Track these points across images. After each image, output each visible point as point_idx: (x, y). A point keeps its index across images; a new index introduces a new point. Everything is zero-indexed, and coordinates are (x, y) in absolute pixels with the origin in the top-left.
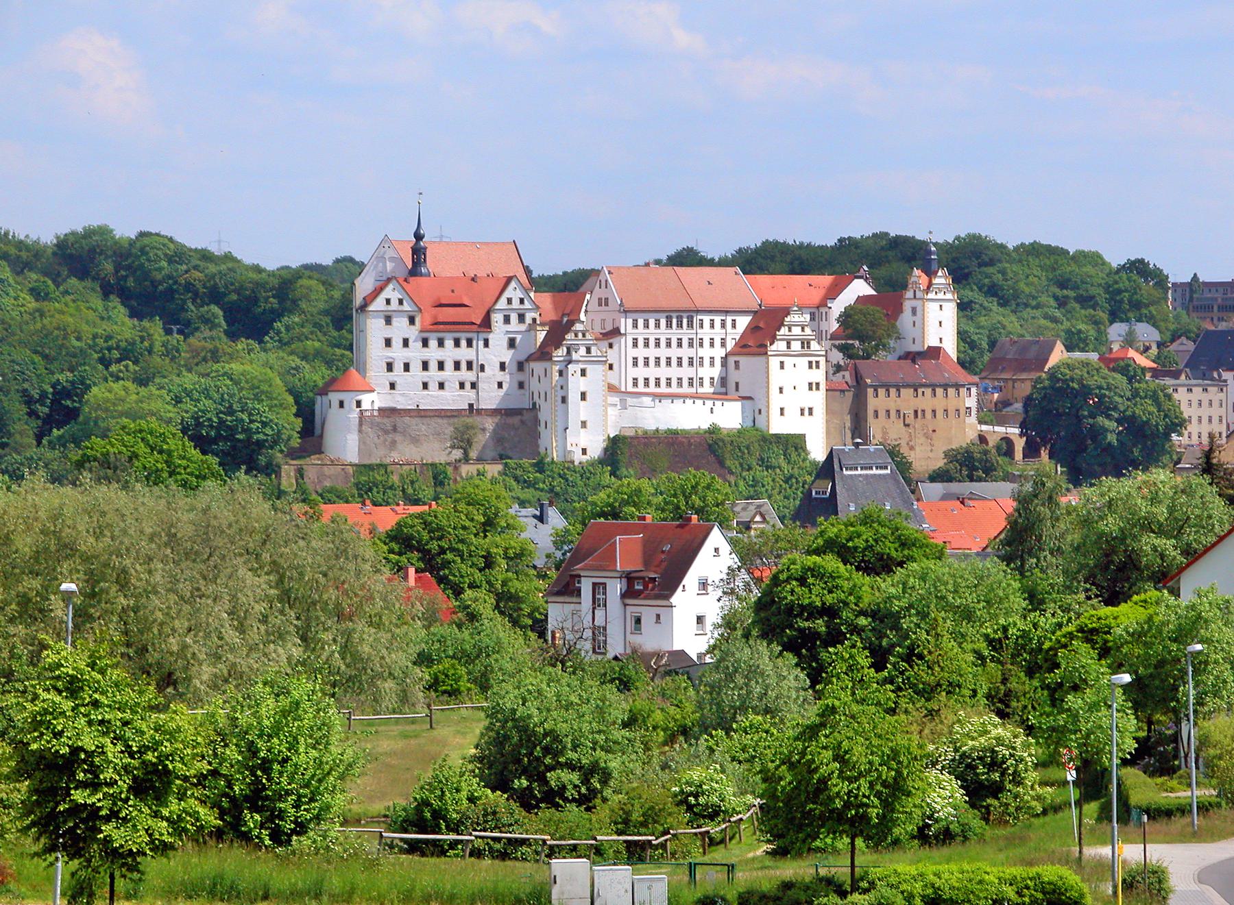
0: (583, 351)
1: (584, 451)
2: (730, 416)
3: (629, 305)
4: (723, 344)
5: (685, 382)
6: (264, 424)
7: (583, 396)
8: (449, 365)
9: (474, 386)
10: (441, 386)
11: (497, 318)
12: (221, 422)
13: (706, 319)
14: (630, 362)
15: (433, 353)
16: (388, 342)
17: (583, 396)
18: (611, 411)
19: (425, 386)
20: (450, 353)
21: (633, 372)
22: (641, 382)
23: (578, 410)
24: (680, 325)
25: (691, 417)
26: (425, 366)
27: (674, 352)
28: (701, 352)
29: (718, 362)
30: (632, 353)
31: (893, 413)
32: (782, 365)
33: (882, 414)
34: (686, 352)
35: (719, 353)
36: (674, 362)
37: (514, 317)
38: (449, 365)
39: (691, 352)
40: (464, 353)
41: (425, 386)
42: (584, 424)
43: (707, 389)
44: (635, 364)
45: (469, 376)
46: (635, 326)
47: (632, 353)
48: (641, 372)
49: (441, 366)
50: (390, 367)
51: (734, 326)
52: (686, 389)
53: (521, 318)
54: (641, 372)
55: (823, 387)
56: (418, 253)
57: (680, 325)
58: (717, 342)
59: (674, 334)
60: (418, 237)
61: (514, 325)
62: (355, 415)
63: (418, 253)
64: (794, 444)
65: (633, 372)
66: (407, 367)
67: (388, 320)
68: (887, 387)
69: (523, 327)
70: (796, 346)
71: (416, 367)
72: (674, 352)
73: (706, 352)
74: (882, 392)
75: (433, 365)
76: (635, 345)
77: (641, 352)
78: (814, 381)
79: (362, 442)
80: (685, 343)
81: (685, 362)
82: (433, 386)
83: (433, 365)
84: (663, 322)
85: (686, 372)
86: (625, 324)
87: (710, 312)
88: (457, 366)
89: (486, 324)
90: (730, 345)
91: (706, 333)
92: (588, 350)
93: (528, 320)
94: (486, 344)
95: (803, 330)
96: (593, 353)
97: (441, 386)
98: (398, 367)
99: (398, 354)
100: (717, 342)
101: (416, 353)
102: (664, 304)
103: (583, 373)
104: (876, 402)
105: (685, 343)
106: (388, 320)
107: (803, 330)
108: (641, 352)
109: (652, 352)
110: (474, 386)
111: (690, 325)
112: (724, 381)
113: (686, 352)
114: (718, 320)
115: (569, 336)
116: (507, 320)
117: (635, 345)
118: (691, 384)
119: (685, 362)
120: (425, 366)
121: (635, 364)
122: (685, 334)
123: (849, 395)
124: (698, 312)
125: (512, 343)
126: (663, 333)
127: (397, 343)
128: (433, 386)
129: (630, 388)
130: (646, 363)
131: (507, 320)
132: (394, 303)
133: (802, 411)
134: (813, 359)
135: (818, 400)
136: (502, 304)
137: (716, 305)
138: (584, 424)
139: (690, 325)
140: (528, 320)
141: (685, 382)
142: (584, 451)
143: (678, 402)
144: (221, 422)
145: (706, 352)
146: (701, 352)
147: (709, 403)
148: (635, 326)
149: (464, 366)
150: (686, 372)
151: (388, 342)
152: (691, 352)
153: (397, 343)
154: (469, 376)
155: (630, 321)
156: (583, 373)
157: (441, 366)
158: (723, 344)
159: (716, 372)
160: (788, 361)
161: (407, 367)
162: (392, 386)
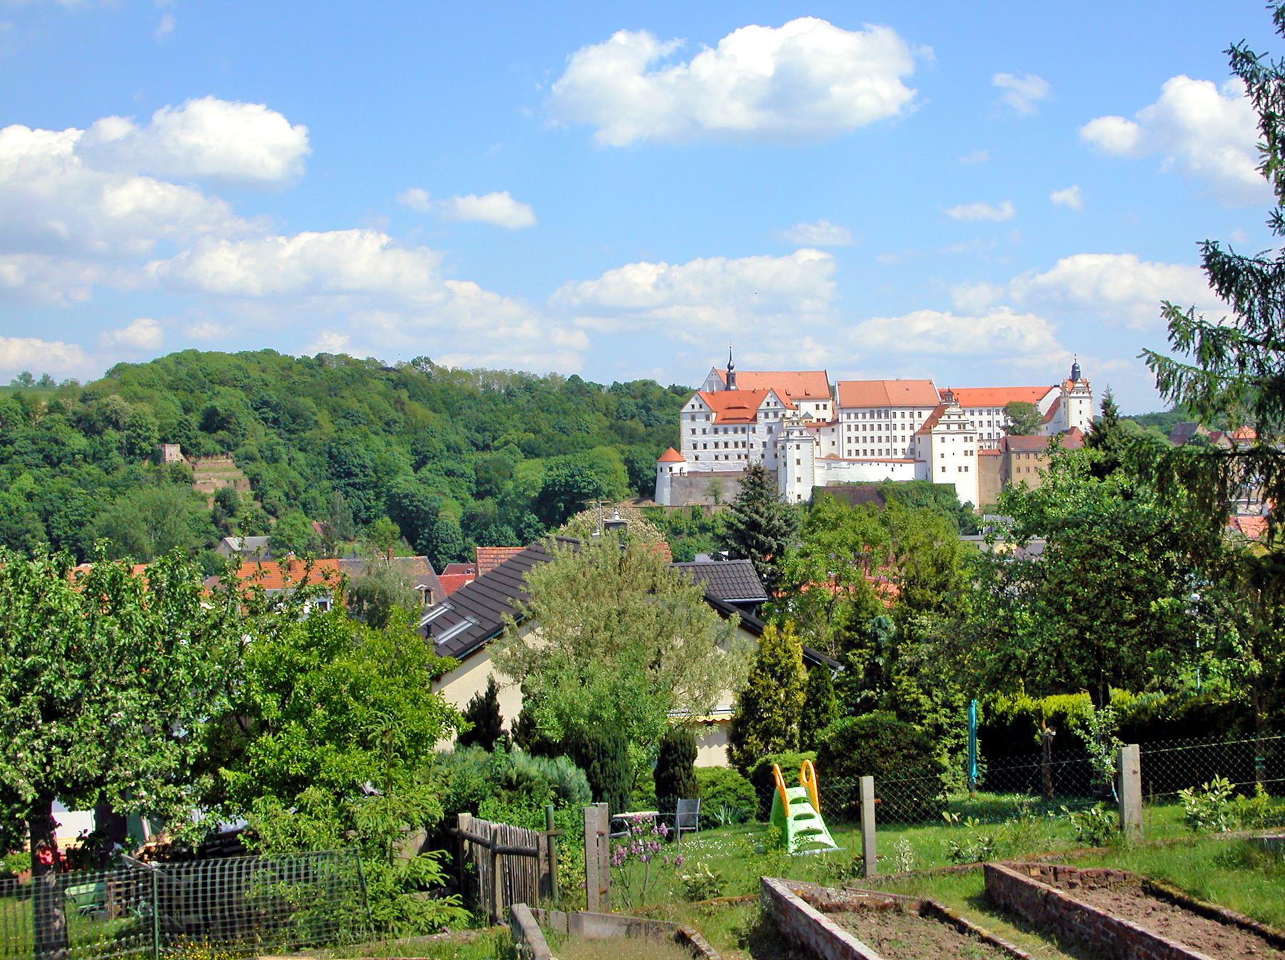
0: (796, 434)
1: (799, 497)
2: (906, 473)
3: (843, 405)
4: (912, 427)
5: (884, 452)
6: (589, 483)
7: (798, 462)
8: (731, 445)
9: (746, 457)
10: (727, 457)
11: (761, 415)
12: (567, 482)
13: (899, 413)
14: (846, 440)
15: (721, 437)
16: (694, 431)
17: (798, 462)
18: (817, 471)
19: (717, 458)
20: (731, 437)
21: (847, 446)
22: (853, 453)
23: (793, 471)
24: (879, 416)
25: (874, 474)
26: (716, 445)
28: (894, 433)
29: (908, 439)
30: (849, 434)
31: (1032, 470)
33: (1023, 470)
35: (908, 433)
36: (876, 439)
37: (771, 415)
38: (731, 445)
39: (888, 433)
40: (740, 437)
41: (717, 458)
42: (799, 479)
43: (900, 455)
45: (741, 450)
46: (849, 417)
47: (849, 434)
48: (853, 446)
49: (726, 445)
50: (695, 447)
51: (920, 415)
52: (884, 456)
53: (776, 415)
54: (853, 446)
55: (975, 453)
56: (730, 378)
57: (879, 416)
58: (907, 427)
59: (876, 421)
60: (730, 368)
61: (771, 419)
62: (668, 476)
63: (730, 378)
64: (949, 490)
65: (847, 446)
66: (705, 446)
67: (693, 419)
68: (1027, 453)
69: (777, 420)
70: (954, 428)
71: (711, 447)
73: (898, 433)
74: (1023, 456)
75: (721, 445)
76: (849, 428)
77: (853, 434)
78: (969, 449)
79: (672, 494)
82: (722, 458)
83: (721, 445)
84: (868, 415)
85: (884, 446)
86: (843, 417)
87: (901, 407)
88: (736, 445)
89: (755, 419)
90: (917, 428)
91: (898, 421)
93: (780, 415)
94: (754, 431)
97: (727, 457)
98: (700, 446)
99: (700, 438)
100: (907, 427)
101: (710, 438)
102: (868, 403)
103: (798, 447)
104: (1015, 462)
106: (693, 419)
108: (853, 434)
109: (861, 434)
110: (746, 457)
111: (886, 415)
112: (912, 451)
113: (884, 433)
114: (907, 413)
116: (767, 416)
117: (849, 428)
118: (888, 453)
119: (884, 439)
120: (716, 445)
123: (1000, 458)
125: (770, 430)
127: (699, 432)
128: (722, 458)
129: (846, 457)
130: (857, 441)
131: (767, 416)
132: (697, 407)
135: (972, 462)
136: (763, 406)
137: (907, 403)
138: (799, 479)
139: (886, 415)
140: (780, 415)
141: (884, 452)
142: (799, 497)
143: (867, 465)
144: (567, 482)
145: (898, 433)
146: (894, 433)
147: (890, 465)
148: (849, 417)
149: (740, 444)
150: (884, 446)
151: (694, 431)
152: (888, 433)
153: (699, 432)
154: (743, 451)
155: (845, 416)
156: (798, 447)
157: (726, 445)
158: (912, 427)
159: (907, 445)
161: (705, 446)
162: (697, 458)
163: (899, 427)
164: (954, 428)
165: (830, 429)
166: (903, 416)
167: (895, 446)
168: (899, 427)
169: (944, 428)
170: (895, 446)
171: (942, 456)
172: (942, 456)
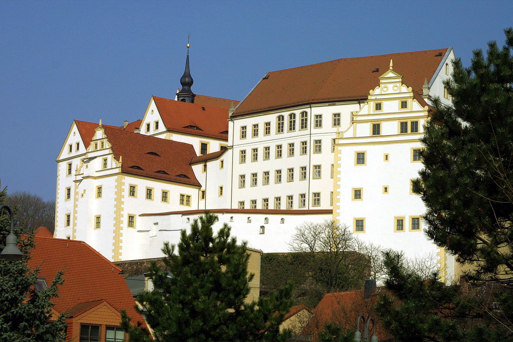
13: (327, 112)
28: (316, 159)
32: (361, 158)
34: (297, 161)
59: (286, 138)
70: (390, 128)
77: (249, 168)
85: (297, 187)
91: (326, 132)
95: (404, 105)
96: (109, 166)
107: (404, 105)
108: (249, 168)
113: (297, 161)
122: (297, 136)
124: (310, 104)
126: (274, 139)
133: (400, 225)
146: (316, 159)
148: (244, 135)
164: (390, 128)
165: (218, 162)
169: (366, 129)
170: (316, 186)
171: (358, 194)
172: (358, 194)
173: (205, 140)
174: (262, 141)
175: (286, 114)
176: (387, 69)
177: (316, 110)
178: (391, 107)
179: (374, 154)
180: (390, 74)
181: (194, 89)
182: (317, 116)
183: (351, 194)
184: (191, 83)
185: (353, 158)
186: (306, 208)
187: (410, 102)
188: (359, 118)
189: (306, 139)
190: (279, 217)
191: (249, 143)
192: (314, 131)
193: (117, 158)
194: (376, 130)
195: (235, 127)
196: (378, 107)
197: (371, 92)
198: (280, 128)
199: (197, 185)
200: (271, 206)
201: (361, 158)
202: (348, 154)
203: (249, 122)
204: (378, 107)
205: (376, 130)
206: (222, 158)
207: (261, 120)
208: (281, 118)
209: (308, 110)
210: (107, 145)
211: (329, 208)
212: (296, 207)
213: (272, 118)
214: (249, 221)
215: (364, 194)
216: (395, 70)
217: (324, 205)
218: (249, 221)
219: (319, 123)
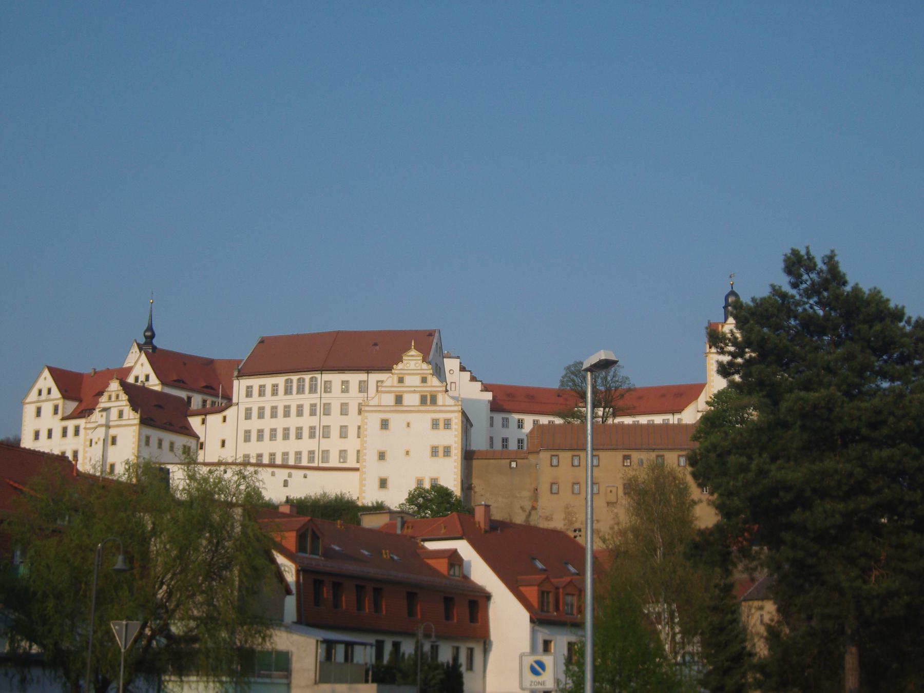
13: (336, 379)
27: (293, 422)
28: (326, 421)
30: (245, 425)
32: (385, 424)
34: (307, 421)
39: (314, 421)
44: (247, 438)
46: (249, 394)
47: (245, 425)
59: (294, 400)
70: (412, 400)
72: (293, 422)
73: (335, 420)
76: (248, 416)
77: (255, 424)
80: (306, 410)
81: (306, 433)
85: (306, 445)
91: (335, 398)
92: (121, 414)
95: (424, 380)
96: (125, 416)
105: (306, 410)
108: (255, 424)
109: (267, 424)
111: (313, 390)
113: (307, 421)
114: (354, 378)
115: (104, 398)
117: (248, 416)
119: (306, 433)
121: (247, 438)
122: (307, 399)
124: (322, 370)
126: (281, 400)
134: (441, 416)
145: (335, 420)
146: (326, 421)
148: (249, 394)
152: (314, 421)
160: (396, 420)
163: (335, 409)
164: (412, 400)
165: (219, 417)
166: (345, 386)
167: (325, 444)
168: (335, 409)
169: (389, 399)
170: (325, 444)
171: (382, 456)
172: (382, 456)
173: (190, 394)
174: (268, 401)
175: (295, 378)
176: (409, 349)
177: (327, 377)
178: (413, 381)
179: (396, 420)
180: (413, 352)
181: (155, 342)
182: (325, 382)
183: (376, 456)
184: (153, 336)
185: (378, 425)
186: (315, 465)
187: (429, 378)
188: (383, 389)
189: (318, 401)
190: (301, 473)
191: (255, 402)
192: (323, 395)
193: (135, 409)
194: (399, 400)
195: (239, 387)
196: (401, 380)
197: (395, 366)
198: (288, 391)
199: (198, 438)
200: (291, 462)
201: (385, 424)
202: (373, 420)
203: (255, 382)
204: (401, 380)
205: (399, 400)
206: (224, 413)
207: (268, 381)
208: (288, 383)
209: (318, 376)
210: (124, 397)
211: (357, 466)
212: (304, 463)
213: (280, 380)
214: (273, 474)
215: (387, 456)
216: (416, 348)
217: (351, 463)
218: (273, 474)
219: (328, 387)
